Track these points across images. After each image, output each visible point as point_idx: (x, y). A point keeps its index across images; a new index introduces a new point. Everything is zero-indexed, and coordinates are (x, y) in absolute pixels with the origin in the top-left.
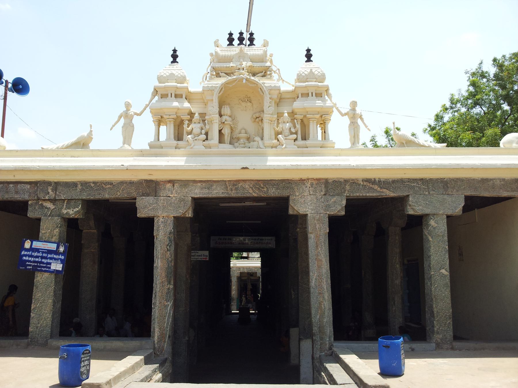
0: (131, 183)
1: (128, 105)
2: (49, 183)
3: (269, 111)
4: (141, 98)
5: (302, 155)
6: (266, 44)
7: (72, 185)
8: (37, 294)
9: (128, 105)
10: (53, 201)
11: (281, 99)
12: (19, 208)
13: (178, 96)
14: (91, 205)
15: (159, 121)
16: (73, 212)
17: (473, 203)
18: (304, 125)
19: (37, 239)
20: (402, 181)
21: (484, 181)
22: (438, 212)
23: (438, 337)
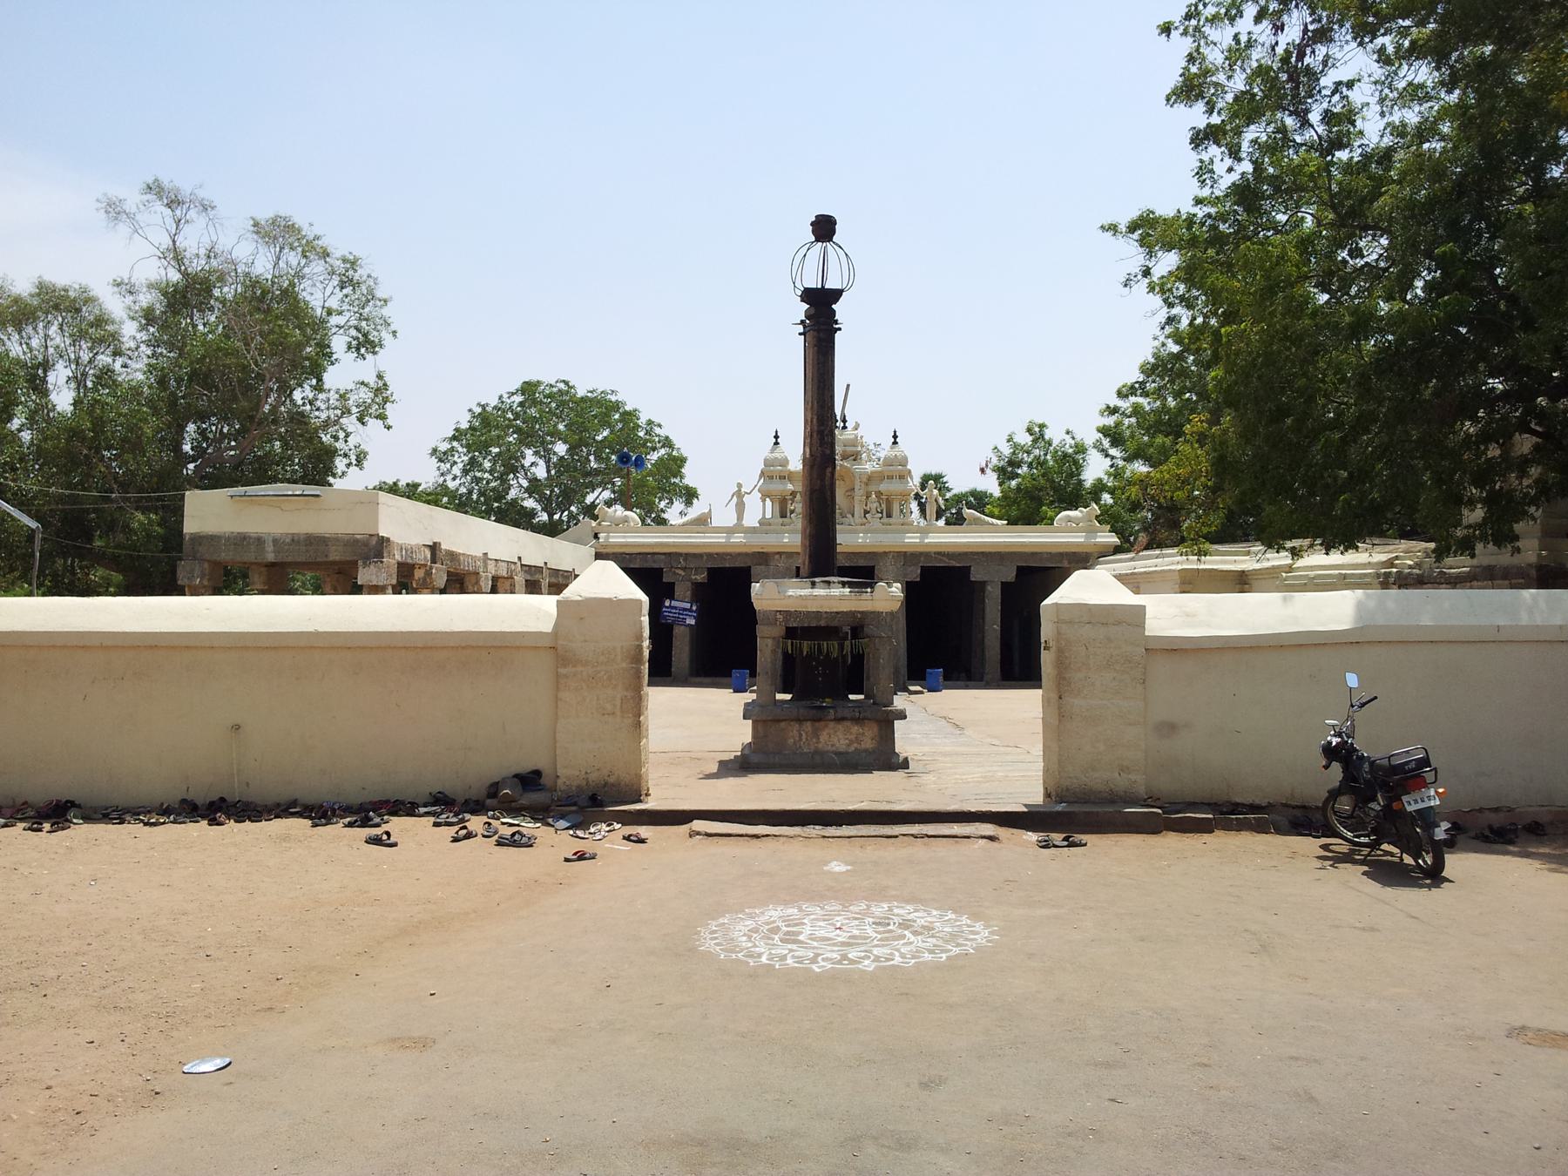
0: (747, 554)
1: (740, 486)
3: (859, 493)
4: (751, 479)
8: (676, 643)
9: (740, 486)
10: (684, 569)
11: (870, 478)
13: (782, 478)
14: (712, 572)
15: (764, 496)
16: (701, 577)
17: (1021, 571)
18: (889, 503)
19: (672, 598)
20: (966, 554)
22: (993, 580)
23: (987, 677)
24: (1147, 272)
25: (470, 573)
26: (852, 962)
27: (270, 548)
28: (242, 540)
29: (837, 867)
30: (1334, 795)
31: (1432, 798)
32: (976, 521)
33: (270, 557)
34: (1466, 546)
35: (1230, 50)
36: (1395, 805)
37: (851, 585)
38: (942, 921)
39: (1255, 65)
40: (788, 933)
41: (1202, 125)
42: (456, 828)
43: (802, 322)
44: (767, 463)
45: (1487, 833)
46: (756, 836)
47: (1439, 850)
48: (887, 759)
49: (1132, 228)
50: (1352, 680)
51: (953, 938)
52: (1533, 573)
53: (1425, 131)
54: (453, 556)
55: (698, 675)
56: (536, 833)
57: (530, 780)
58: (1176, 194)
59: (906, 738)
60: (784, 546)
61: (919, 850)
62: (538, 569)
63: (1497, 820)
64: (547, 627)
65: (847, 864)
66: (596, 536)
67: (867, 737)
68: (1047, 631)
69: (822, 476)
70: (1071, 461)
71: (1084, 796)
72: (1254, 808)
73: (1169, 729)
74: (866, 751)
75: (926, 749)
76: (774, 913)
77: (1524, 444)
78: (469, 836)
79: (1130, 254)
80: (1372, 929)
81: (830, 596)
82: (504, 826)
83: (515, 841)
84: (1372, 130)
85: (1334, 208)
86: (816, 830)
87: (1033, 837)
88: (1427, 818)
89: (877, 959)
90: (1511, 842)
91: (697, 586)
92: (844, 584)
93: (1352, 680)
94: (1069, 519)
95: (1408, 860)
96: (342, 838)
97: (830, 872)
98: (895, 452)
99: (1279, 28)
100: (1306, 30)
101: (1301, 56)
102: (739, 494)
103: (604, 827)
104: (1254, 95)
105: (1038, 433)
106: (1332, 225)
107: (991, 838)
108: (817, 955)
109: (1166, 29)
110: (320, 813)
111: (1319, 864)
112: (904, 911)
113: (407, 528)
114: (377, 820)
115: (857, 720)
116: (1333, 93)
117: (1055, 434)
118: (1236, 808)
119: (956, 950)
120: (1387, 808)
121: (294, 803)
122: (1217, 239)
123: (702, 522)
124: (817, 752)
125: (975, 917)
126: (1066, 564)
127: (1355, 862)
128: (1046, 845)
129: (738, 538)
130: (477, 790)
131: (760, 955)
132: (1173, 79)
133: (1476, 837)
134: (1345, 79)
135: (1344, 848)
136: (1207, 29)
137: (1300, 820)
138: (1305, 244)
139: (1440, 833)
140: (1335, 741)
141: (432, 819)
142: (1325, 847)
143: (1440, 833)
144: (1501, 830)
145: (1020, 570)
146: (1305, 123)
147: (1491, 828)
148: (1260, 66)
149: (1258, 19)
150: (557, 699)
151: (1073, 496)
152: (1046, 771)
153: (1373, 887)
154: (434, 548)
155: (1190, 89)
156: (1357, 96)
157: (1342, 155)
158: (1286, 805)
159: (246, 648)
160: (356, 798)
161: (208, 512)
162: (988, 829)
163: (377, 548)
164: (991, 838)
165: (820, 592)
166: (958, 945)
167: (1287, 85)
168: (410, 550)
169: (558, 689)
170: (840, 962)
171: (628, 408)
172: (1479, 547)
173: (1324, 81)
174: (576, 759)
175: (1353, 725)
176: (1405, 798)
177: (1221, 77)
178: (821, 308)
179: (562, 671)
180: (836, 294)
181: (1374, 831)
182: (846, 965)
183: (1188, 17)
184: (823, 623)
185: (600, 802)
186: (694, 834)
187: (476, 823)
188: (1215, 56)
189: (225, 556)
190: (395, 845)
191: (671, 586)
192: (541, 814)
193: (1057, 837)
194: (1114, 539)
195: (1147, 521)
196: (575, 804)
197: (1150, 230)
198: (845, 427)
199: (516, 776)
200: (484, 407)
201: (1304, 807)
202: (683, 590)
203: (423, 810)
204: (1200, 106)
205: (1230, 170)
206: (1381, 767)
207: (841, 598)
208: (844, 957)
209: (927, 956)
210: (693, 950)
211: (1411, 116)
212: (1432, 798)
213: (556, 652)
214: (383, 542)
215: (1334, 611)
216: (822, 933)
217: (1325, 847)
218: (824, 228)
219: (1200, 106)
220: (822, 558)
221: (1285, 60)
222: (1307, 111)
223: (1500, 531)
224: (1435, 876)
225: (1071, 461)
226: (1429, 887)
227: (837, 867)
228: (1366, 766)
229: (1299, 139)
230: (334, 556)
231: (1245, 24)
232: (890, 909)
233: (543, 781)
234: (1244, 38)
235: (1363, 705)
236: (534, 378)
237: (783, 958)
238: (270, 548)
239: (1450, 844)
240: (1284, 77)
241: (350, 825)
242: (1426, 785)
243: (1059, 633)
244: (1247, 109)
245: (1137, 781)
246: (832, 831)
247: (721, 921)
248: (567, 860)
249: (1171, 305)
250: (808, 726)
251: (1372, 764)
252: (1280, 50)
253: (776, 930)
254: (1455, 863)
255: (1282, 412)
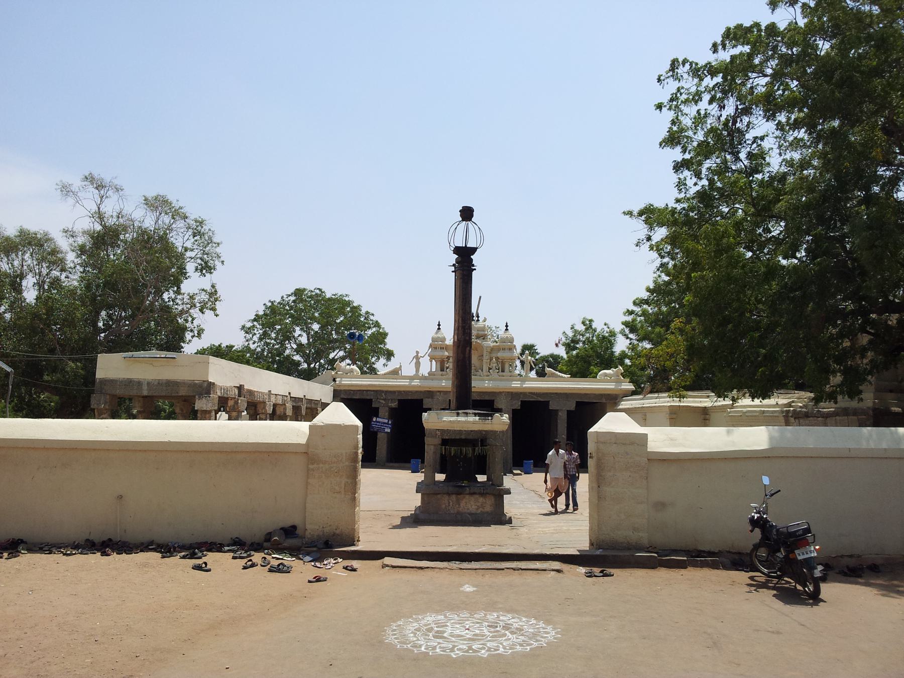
0: (421, 392)
1: (417, 352)
2: (382, 391)
4: (424, 349)
5: (501, 380)
6: (485, 320)
7: (394, 392)
8: (379, 443)
9: (417, 352)
10: (384, 400)
11: (492, 350)
12: (370, 401)
13: (442, 348)
14: (401, 402)
15: (432, 358)
16: (394, 405)
18: (503, 364)
19: (377, 416)
20: (547, 394)
21: (586, 394)
22: (563, 409)
24: (649, 239)
25: (260, 402)
26: (475, 651)
27: (145, 387)
28: (129, 383)
29: (468, 588)
30: (756, 547)
31: (813, 551)
32: (553, 375)
33: (145, 393)
34: (832, 397)
35: (695, 118)
36: (791, 556)
37: (479, 415)
38: (528, 624)
39: (709, 127)
40: (437, 632)
41: (680, 160)
42: (246, 560)
43: (454, 265)
44: (434, 340)
45: (846, 570)
46: (421, 568)
47: (817, 582)
48: (499, 518)
49: (641, 213)
50: (766, 480)
51: (534, 636)
52: (871, 413)
53: (804, 164)
54: (251, 392)
55: (391, 462)
56: (292, 564)
57: (290, 531)
58: (666, 196)
59: (511, 505)
60: (443, 387)
61: (516, 578)
62: (300, 400)
63: (852, 562)
64: (303, 441)
65: (474, 586)
66: (334, 380)
67: (488, 504)
68: (591, 447)
69: (464, 352)
70: (607, 340)
71: (613, 545)
72: (711, 554)
73: (661, 506)
74: (487, 512)
75: (523, 511)
76: (430, 618)
77: (864, 339)
78: (253, 565)
79: (639, 228)
80: (778, 633)
81: (468, 421)
82: (274, 559)
83: (280, 569)
84: (775, 163)
85: (754, 206)
86: (455, 565)
87: (582, 570)
88: (809, 563)
89: (489, 650)
90: (860, 576)
91: (392, 410)
92: (475, 414)
93: (766, 480)
94: (606, 375)
95: (799, 587)
96: (179, 566)
97: (463, 591)
98: (507, 335)
99: (722, 107)
100: (737, 109)
101: (735, 122)
102: (417, 357)
103: (332, 561)
104: (709, 143)
105: (588, 325)
106: (753, 215)
107: (558, 571)
108: (454, 646)
109: (659, 107)
110: (166, 549)
111: (747, 589)
112: (506, 618)
113: (224, 375)
114: (200, 554)
115: (482, 494)
116: (753, 143)
117: (598, 326)
118: (700, 553)
119: (535, 644)
120: (786, 557)
121: (152, 543)
122: (689, 222)
123: (395, 373)
124: (458, 513)
125: (548, 622)
126: (604, 401)
127: (769, 588)
128: (590, 575)
129: (416, 383)
130: (259, 537)
131: (421, 646)
132: (663, 134)
133: (839, 573)
134: (759, 136)
135: (763, 579)
136: (682, 107)
137: (737, 561)
138: (738, 225)
139: (818, 572)
140: (756, 516)
141: (232, 554)
142: (751, 578)
143: (818, 572)
144: (854, 569)
145: (577, 403)
146: (738, 159)
147: (848, 567)
148: (712, 128)
149: (710, 102)
150: (307, 484)
151: (609, 361)
152: (591, 529)
153: (779, 605)
154: (240, 388)
155: (673, 139)
156: (766, 144)
157: (759, 176)
158: (729, 552)
159: (128, 450)
160: (188, 541)
161: (111, 366)
162: (556, 565)
163: (207, 388)
164: (558, 571)
165: (461, 419)
166: (537, 641)
167: (727, 138)
168: (226, 390)
169: (308, 478)
170: (467, 651)
171: (355, 305)
172: (840, 398)
173: (748, 136)
174: (317, 519)
175: (766, 506)
176: (797, 552)
177: (690, 133)
178: (464, 258)
179: (311, 467)
180: (473, 250)
181: (779, 570)
182: (471, 653)
183: (672, 100)
184: (463, 437)
185: (329, 544)
186: (384, 566)
187: (257, 557)
188: (687, 122)
189: (119, 392)
190: (209, 570)
191: (377, 409)
192: (295, 552)
193: (597, 570)
194: (631, 387)
195: (650, 377)
196: (315, 546)
197: (650, 215)
198: (478, 320)
199: (282, 529)
200: (272, 303)
201: (740, 553)
202: (384, 412)
203: (227, 548)
204: (678, 149)
205: (695, 184)
206: (782, 533)
207: (474, 423)
208: (470, 648)
209: (519, 648)
210: (381, 642)
211: (796, 156)
212: (813, 551)
213: (307, 455)
214: (211, 385)
215: (756, 438)
216: (458, 632)
217: (751, 578)
218: (467, 214)
219: (678, 149)
220: (463, 398)
221: (726, 124)
222: (739, 152)
223: (852, 390)
224: (815, 598)
225: (607, 340)
226: (812, 605)
227: (468, 588)
228: (774, 530)
229: (734, 168)
230: (183, 392)
231: (704, 105)
232: (498, 617)
233: (297, 532)
234: (703, 112)
235: (772, 495)
236: (302, 287)
237: (434, 648)
238: (145, 387)
239: (824, 579)
240: (725, 133)
241: (184, 557)
242: (808, 544)
243: (598, 449)
244: (704, 150)
245: (643, 537)
246: (465, 565)
247: (399, 623)
248: (310, 582)
249: (662, 257)
250: (454, 497)
251: (778, 530)
252: (723, 119)
253: (430, 630)
254: (827, 590)
255: (726, 321)
